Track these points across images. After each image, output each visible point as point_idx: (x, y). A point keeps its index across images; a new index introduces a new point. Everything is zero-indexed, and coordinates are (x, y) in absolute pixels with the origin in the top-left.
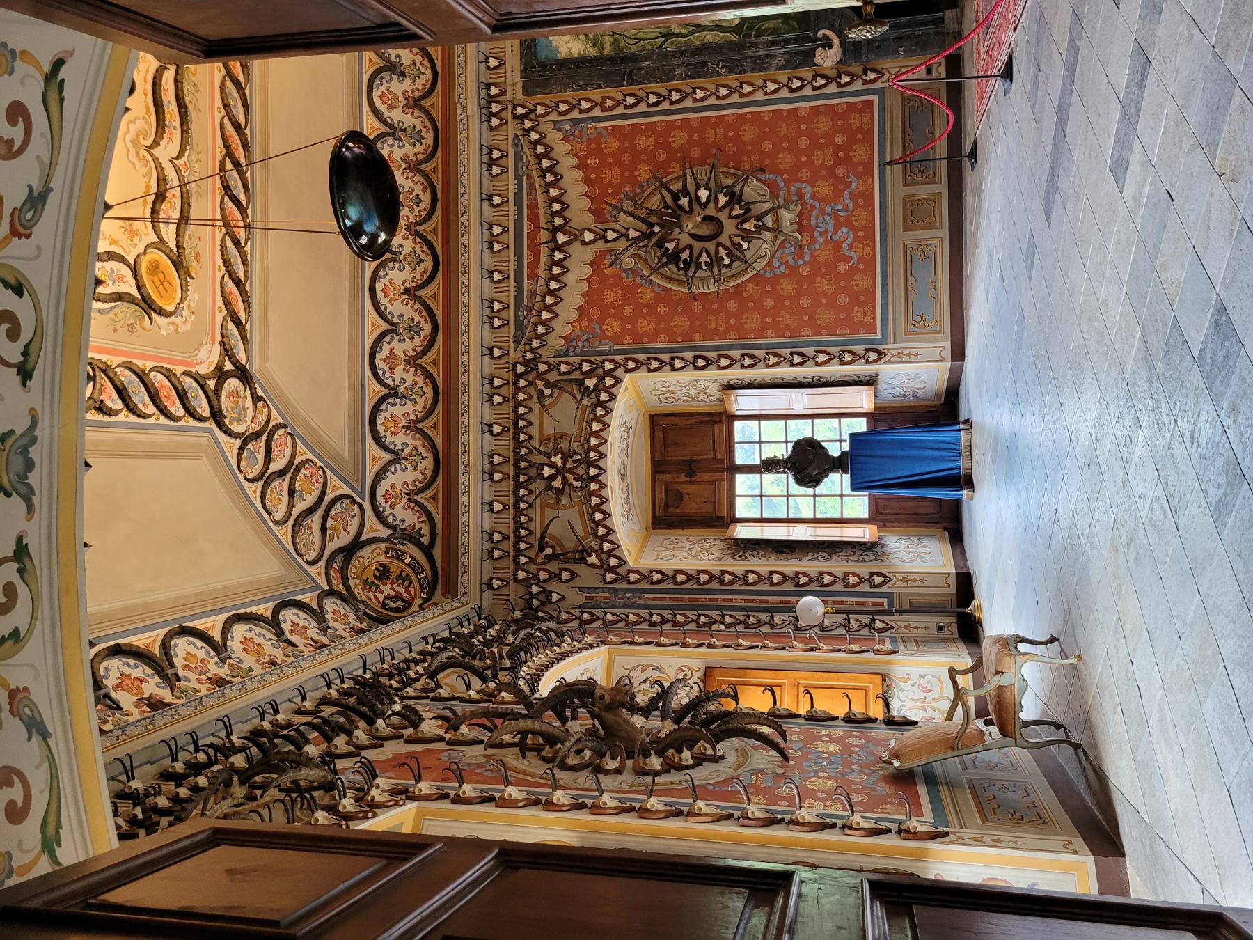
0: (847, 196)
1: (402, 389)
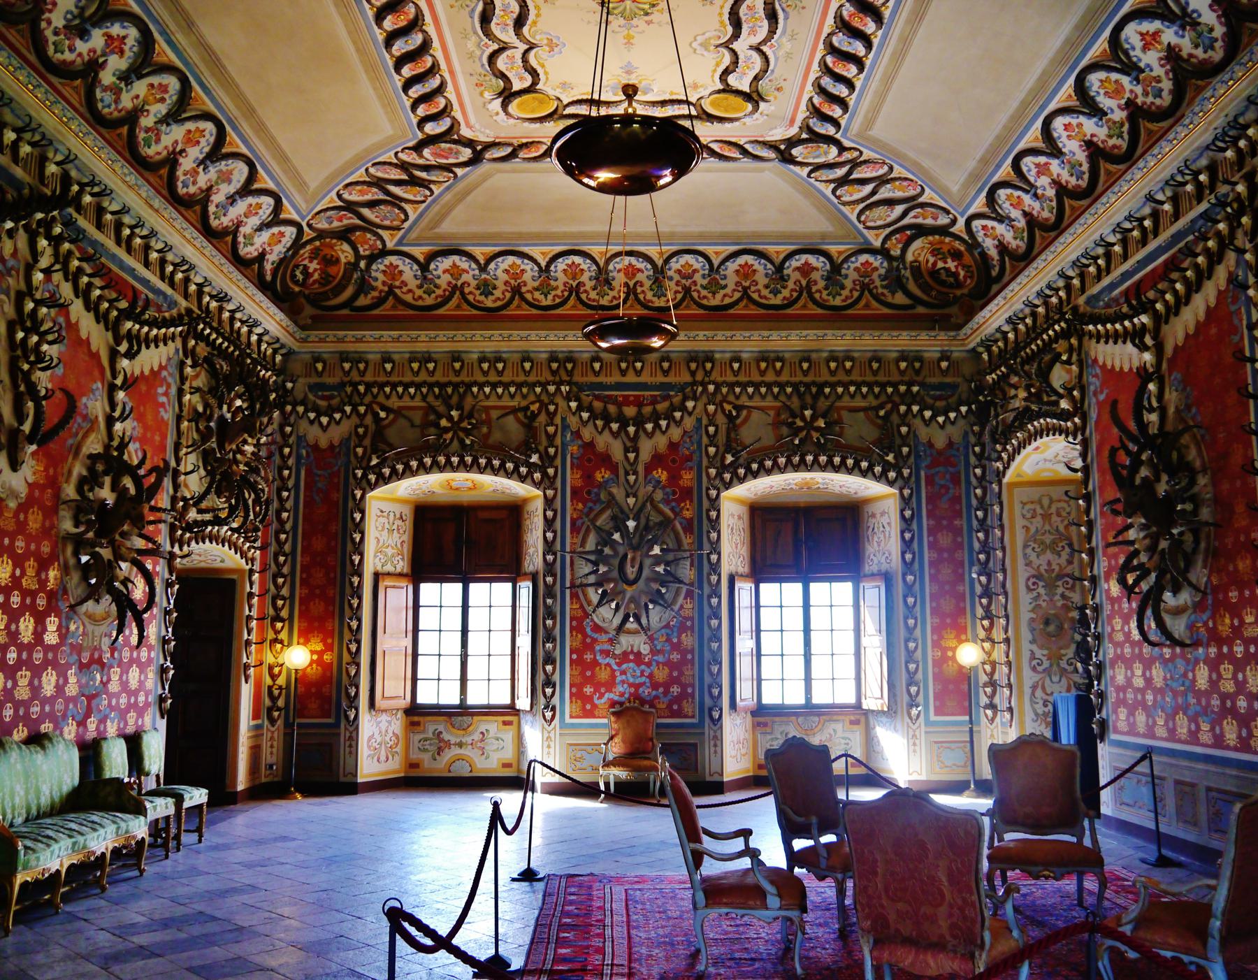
0: (1198, 708)
1: (1040, 192)
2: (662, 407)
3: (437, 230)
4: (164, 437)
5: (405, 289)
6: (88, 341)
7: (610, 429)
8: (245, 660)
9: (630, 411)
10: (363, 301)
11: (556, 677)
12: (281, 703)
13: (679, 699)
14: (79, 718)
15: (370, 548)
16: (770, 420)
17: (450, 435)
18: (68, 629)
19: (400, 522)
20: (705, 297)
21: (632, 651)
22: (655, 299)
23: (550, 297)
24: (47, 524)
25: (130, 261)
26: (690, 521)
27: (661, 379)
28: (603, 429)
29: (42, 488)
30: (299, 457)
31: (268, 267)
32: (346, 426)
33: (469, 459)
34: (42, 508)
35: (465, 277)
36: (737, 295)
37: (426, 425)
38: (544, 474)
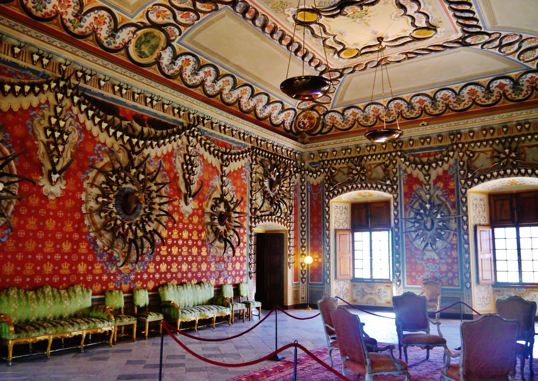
2: (438, 156)
4: (245, 189)
6: (211, 164)
7: (418, 168)
8: (289, 261)
9: (425, 159)
10: (325, 130)
11: (401, 269)
12: (305, 276)
13: (452, 279)
14: (216, 278)
15: (332, 220)
16: (489, 156)
17: (357, 176)
18: (210, 251)
19: (345, 210)
20: (456, 107)
21: (431, 259)
22: (434, 111)
23: (391, 118)
24: (200, 220)
25: (226, 136)
26: (454, 203)
27: (439, 144)
28: (415, 168)
29: (198, 210)
30: (308, 189)
31: (288, 125)
32: (322, 176)
33: (364, 185)
34: (198, 215)
35: (358, 116)
36: (470, 103)
37: (349, 173)
38: (393, 188)
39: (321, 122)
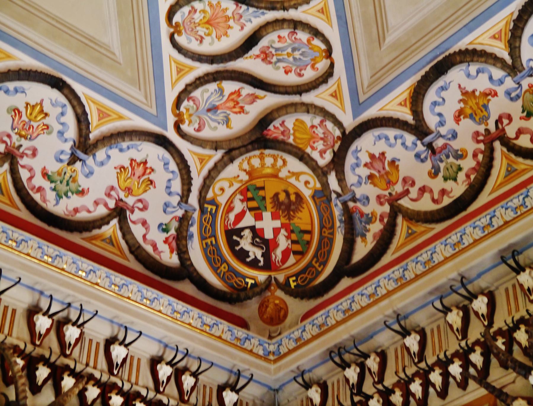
3: (390, 39)
5: (414, 192)
39: (337, 211)
